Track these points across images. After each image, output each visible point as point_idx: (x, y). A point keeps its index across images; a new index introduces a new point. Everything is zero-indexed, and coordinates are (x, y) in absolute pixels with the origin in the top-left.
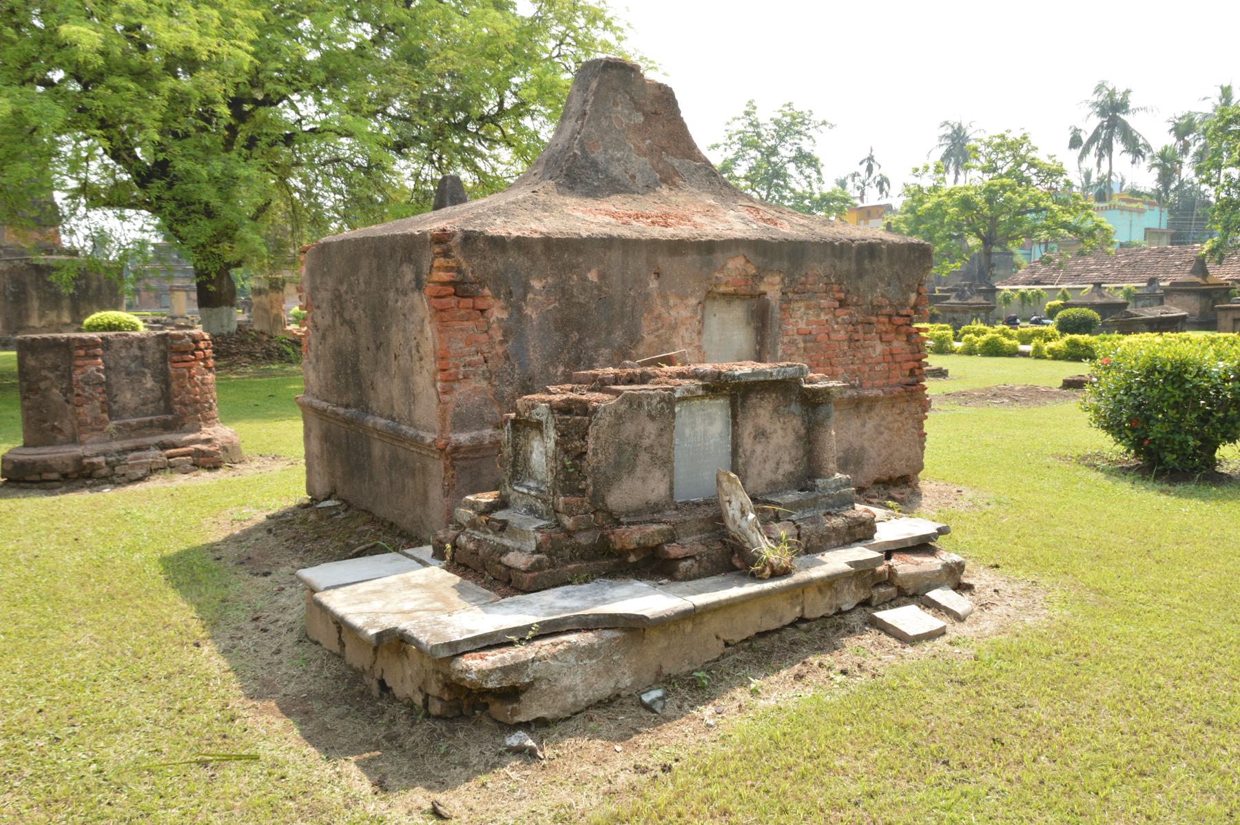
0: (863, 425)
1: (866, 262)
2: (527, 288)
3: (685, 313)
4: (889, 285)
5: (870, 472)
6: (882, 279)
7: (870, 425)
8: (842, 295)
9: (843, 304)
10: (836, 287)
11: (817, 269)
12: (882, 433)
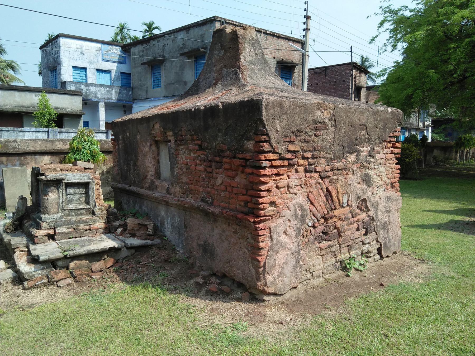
0: (213, 230)
1: (209, 120)
2: (119, 138)
3: (147, 149)
4: (226, 134)
5: (219, 266)
6: (220, 130)
7: (216, 232)
8: (199, 142)
9: (201, 148)
10: (195, 137)
11: (185, 127)
12: (223, 241)
